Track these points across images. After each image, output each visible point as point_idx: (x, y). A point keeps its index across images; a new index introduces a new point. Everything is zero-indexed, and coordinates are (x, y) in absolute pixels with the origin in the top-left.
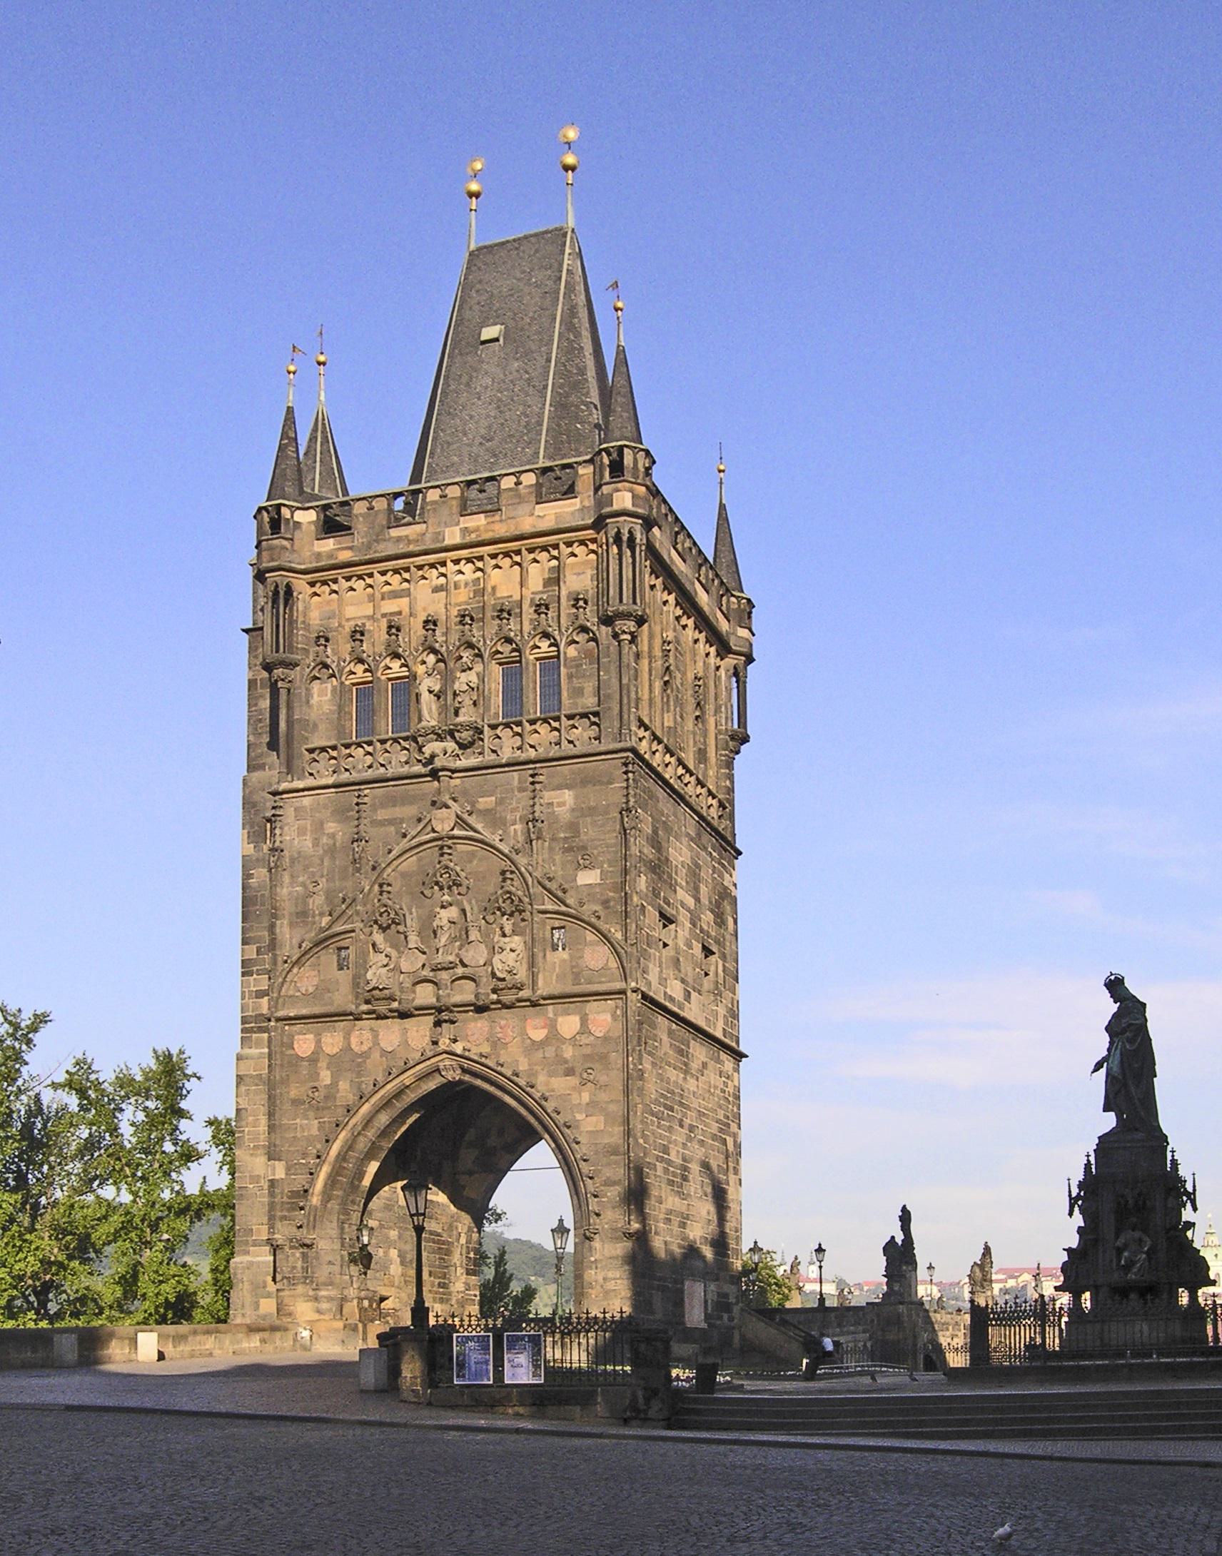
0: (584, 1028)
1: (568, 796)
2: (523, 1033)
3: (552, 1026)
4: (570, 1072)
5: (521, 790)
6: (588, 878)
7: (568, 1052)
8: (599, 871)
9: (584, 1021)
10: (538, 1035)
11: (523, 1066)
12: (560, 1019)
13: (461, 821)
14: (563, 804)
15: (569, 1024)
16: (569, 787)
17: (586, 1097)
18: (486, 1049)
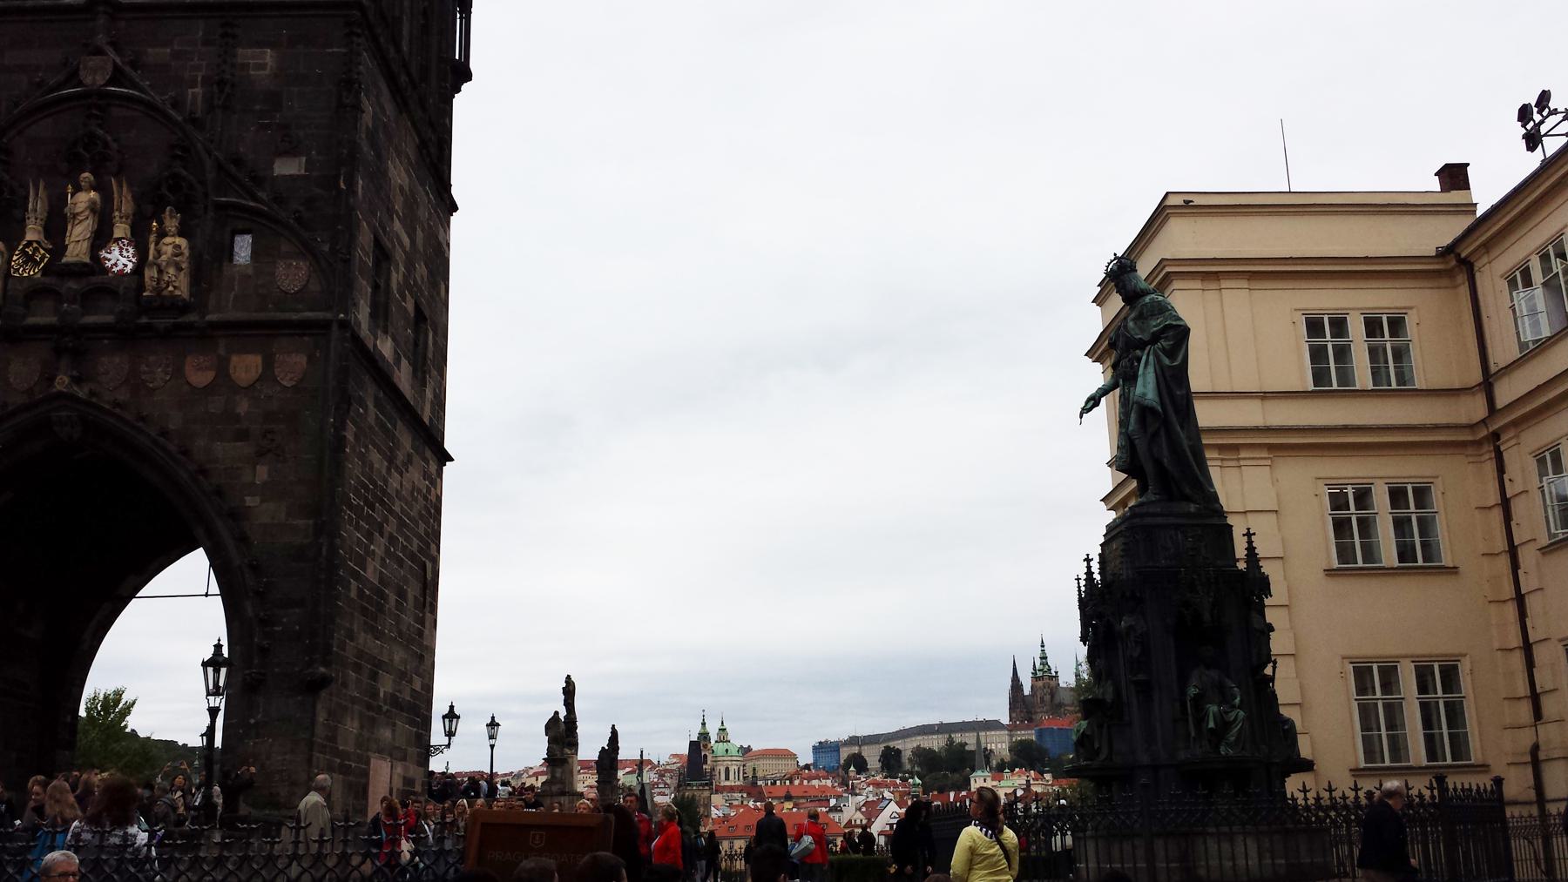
0: (267, 375)
1: (269, 56)
2: (179, 372)
3: (222, 369)
4: (242, 436)
5: (206, 43)
6: (287, 168)
7: (243, 407)
8: (304, 159)
9: (268, 363)
10: (200, 377)
11: (175, 422)
12: (235, 359)
13: (118, 77)
14: (263, 67)
15: (246, 367)
16: (271, 45)
17: (262, 473)
18: (123, 396)
